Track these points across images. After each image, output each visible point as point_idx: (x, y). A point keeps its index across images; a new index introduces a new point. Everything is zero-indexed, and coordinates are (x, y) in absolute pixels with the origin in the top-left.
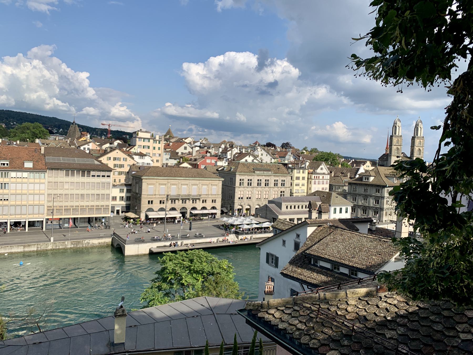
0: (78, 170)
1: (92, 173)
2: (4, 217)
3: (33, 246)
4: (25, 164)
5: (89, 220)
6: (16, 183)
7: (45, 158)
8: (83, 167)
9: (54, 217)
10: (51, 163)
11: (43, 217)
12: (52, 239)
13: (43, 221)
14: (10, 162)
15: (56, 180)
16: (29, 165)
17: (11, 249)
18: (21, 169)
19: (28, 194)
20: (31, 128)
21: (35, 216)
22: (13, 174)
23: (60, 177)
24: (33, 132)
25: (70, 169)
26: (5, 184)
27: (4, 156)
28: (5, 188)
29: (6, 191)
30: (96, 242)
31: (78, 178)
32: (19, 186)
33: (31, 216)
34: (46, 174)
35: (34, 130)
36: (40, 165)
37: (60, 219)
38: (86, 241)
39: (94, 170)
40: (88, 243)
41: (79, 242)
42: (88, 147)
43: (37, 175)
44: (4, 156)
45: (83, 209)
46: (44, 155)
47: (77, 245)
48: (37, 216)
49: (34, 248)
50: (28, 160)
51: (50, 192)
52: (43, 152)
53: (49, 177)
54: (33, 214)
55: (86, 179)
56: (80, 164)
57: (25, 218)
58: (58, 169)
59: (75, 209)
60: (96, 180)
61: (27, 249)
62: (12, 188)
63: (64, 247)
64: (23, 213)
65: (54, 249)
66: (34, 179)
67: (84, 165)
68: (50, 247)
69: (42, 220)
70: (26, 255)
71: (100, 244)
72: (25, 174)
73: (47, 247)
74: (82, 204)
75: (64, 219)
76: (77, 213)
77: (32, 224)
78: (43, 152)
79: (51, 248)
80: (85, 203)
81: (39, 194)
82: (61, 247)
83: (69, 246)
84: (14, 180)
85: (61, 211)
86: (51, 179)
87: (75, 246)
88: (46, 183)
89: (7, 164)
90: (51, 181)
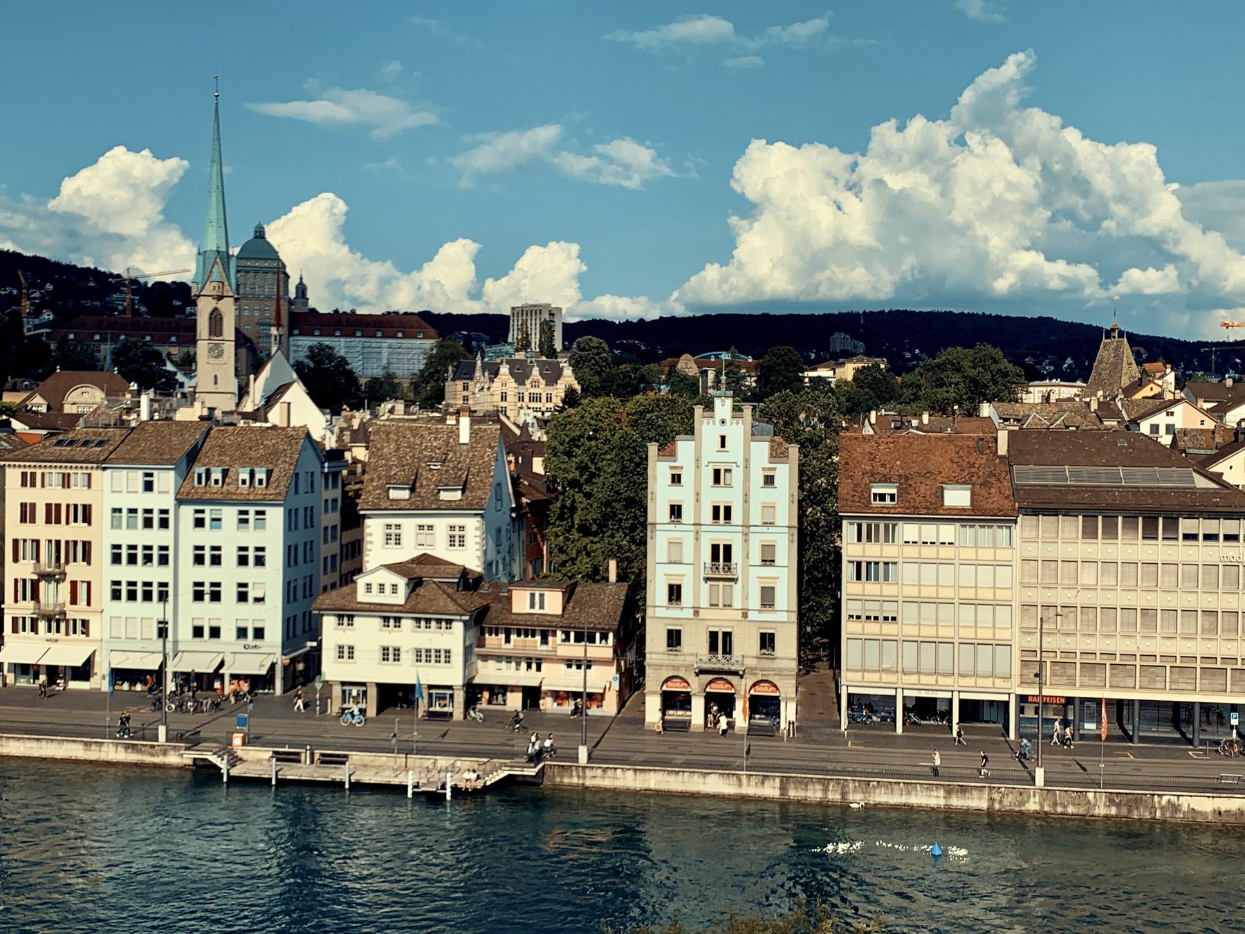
0: (1130, 518)
1: (1185, 525)
2: (886, 678)
3: (975, 793)
4: (947, 494)
5: (1178, 714)
6: (920, 562)
7: (1011, 472)
8: (1150, 502)
9: (1046, 692)
10: (1033, 490)
11: (1005, 686)
12: (1040, 774)
13: (1007, 704)
14: (899, 489)
15: (1051, 551)
16: (957, 497)
17: (909, 793)
18: (934, 512)
19: (957, 601)
20: (966, 364)
21: (981, 682)
22: (909, 531)
23: (1062, 538)
24: (974, 381)
25: (1097, 511)
26: (886, 564)
27: (881, 470)
28: (886, 578)
29: (889, 590)
30: (1205, 805)
31: (1129, 547)
32: (928, 571)
33: (969, 682)
34: (1017, 530)
35: (973, 373)
36: (996, 499)
37: (1070, 700)
38: (1165, 799)
39: (1191, 515)
40: (1175, 808)
41: (1138, 801)
42: (1170, 420)
43: (985, 533)
44: (881, 470)
45: (1151, 667)
46: (1008, 461)
47: (1130, 811)
48: (988, 682)
49: (977, 801)
50: (957, 481)
51: (1033, 596)
52: (1002, 449)
53: (1024, 540)
54: (975, 675)
55: (1160, 550)
56: (1136, 491)
57: (954, 688)
58: (1054, 512)
59: (1122, 667)
60: (1202, 552)
61: (957, 802)
62: (908, 581)
63: (1081, 810)
64: (941, 668)
65: (1046, 813)
66: (976, 546)
67: (1151, 492)
68: (1032, 805)
69: (1004, 698)
70: (955, 824)
71: (1224, 819)
72: (948, 532)
73: (1022, 803)
74: (1147, 646)
75: (1083, 700)
76: (1130, 682)
77: (972, 710)
78: (1002, 449)
79: (1036, 807)
80: (1159, 647)
81: (994, 604)
82: (1071, 810)
83: (1101, 811)
84: (911, 551)
85: (1070, 672)
86: (1032, 550)
87: (1124, 811)
88: (1017, 564)
89: (892, 497)
90: (1032, 555)
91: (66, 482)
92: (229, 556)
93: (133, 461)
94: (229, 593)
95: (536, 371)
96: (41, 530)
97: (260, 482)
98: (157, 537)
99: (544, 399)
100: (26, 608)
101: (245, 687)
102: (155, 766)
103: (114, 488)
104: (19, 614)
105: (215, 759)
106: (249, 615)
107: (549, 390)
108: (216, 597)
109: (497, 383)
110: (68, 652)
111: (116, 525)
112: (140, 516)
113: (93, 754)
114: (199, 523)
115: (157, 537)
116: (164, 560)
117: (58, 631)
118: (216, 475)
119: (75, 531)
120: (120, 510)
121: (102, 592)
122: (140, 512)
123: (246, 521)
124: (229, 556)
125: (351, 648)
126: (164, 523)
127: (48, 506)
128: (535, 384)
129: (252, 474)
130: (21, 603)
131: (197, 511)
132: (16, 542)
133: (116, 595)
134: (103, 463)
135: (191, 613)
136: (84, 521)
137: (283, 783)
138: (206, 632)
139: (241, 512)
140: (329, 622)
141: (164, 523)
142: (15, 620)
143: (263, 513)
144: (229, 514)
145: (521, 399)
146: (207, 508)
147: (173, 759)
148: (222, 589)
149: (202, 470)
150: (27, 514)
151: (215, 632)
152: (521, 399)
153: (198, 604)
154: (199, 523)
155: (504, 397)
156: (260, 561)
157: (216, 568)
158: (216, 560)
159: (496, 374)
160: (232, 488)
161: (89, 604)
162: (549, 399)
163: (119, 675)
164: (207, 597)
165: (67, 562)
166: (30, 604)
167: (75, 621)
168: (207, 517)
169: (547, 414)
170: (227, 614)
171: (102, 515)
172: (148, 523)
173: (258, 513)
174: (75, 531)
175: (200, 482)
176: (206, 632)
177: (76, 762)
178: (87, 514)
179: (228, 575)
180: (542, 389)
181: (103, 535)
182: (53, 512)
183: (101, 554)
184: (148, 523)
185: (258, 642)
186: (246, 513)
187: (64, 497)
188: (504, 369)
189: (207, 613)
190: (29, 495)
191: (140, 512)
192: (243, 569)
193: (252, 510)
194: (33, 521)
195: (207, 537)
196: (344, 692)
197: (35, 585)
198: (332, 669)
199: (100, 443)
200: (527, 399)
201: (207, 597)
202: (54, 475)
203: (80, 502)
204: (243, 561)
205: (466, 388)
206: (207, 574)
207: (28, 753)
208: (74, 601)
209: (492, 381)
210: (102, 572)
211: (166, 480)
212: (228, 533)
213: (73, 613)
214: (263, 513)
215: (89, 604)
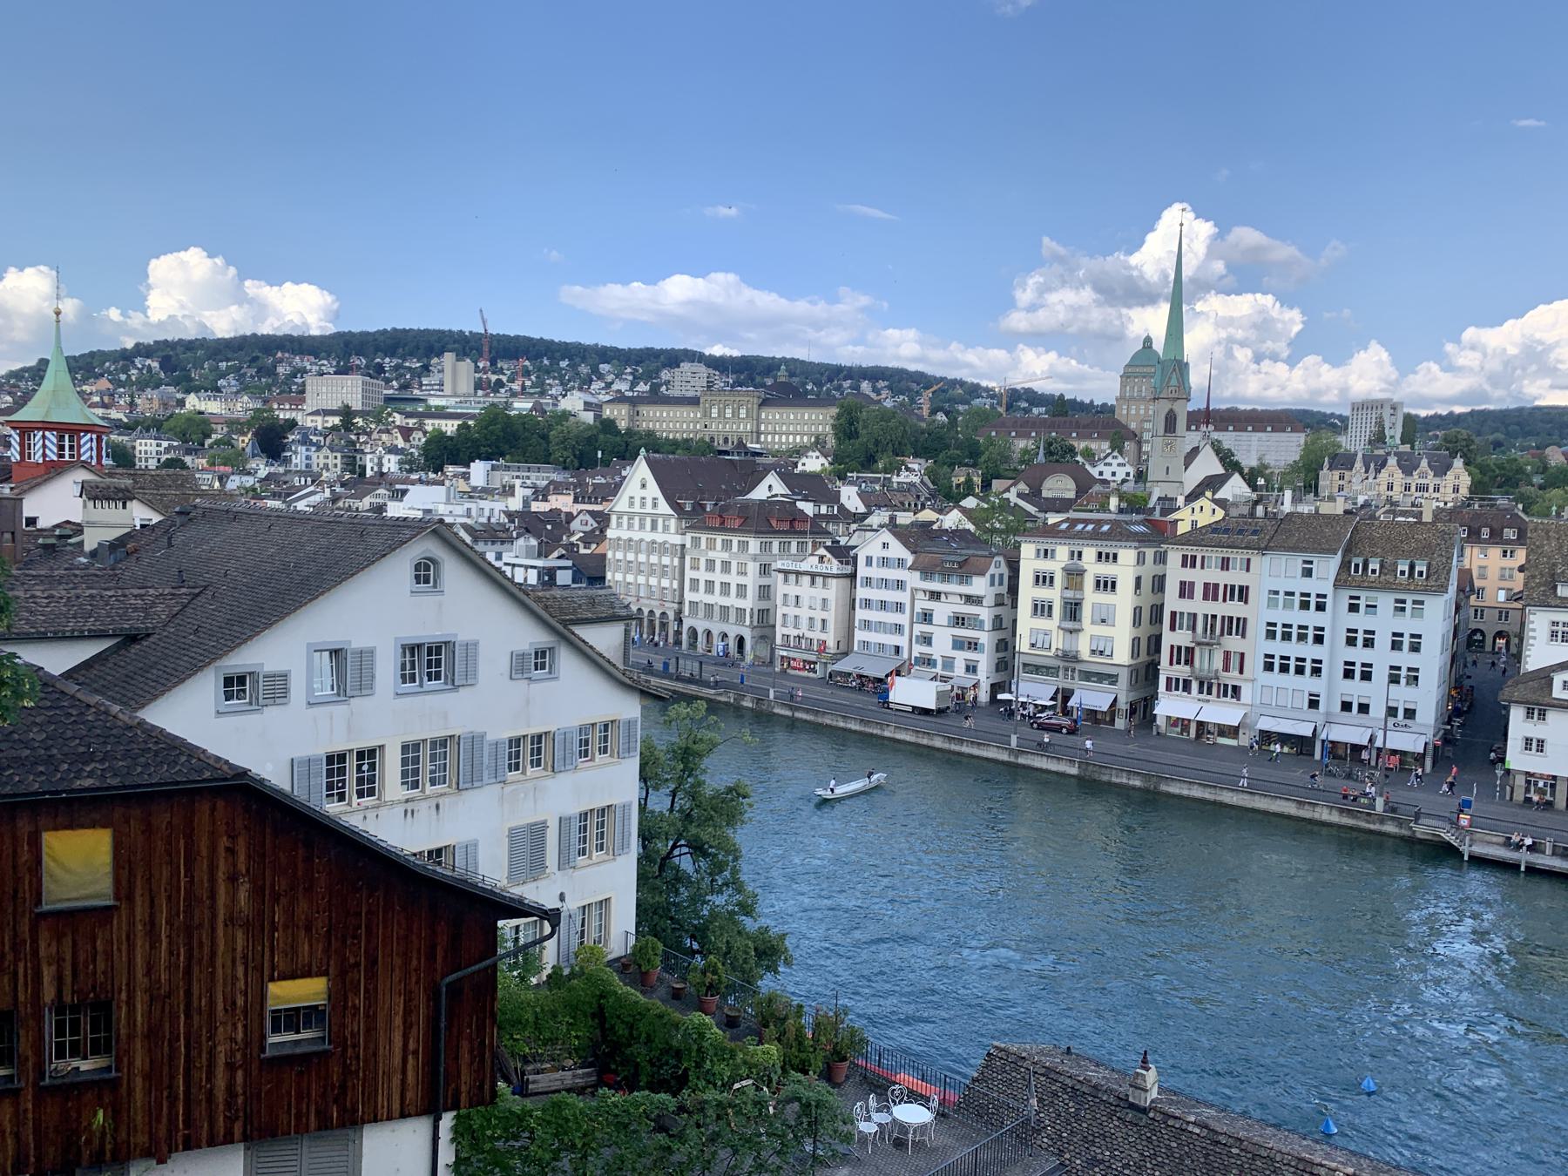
91: (1225, 564)
92: (1383, 640)
93: (1294, 549)
94: (1380, 674)
95: (1424, 463)
96: (1199, 606)
97: (1421, 574)
98: (1312, 618)
99: (1431, 489)
100: (1181, 671)
101: (1395, 760)
102: (1371, 832)
103: (1272, 574)
104: (1174, 675)
105: (1448, 837)
106: (1402, 695)
107: (1437, 481)
108: (1366, 676)
109: (1384, 474)
110: (1221, 712)
111: (1272, 604)
112: (1297, 599)
113: (1306, 813)
114: (1354, 608)
115: (1312, 618)
116: (1319, 639)
117: (1209, 693)
118: (1374, 565)
119: (1234, 609)
120: (1276, 593)
121: (1254, 664)
122: (1297, 595)
123: (1403, 609)
124: (1383, 640)
125: (1541, 743)
126: (1321, 607)
127: (1206, 585)
128: (1423, 475)
129: (1412, 567)
130: (1176, 667)
131: (1352, 598)
132: (1173, 614)
133: (1269, 667)
134: (1263, 549)
135: (1334, 688)
136: (1240, 599)
137: (1532, 870)
138: (1355, 708)
139: (1397, 601)
140: (1517, 715)
141: (1321, 607)
142: (1169, 680)
143: (1422, 603)
144: (1386, 601)
145: (1408, 488)
146: (1363, 594)
147: (1390, 828)
148: (1420, 675)
149: (1360, 561)
150: (1186, 590)
151: (1364, 708)
152: (1408, 488)
153: (1348, 682)
154: (1354, 608)
155: (1390, 487)
156: (1415, 648)
157: (1368, 650)
158: (1369, 643)
159: (1384, 464)
160: (1390, 578)
161: (1241, 672)
162: (1436, 489)
163: (1267, 737)
164: (1403, 681)
165: (1222, 634)
166: (1187, 668)
167: (1226, 686)
168: (1362, 603)
169: (1450, 505)
170: (1376, 692)
171: (1258, 596)
172: (1305, 605)
173: (1415, 602)
174: (1234, 609)
175: (1356, 571)
176: (1355, 708)
177: (1289, 817)
178: (1243, 594)
179: (1381, 658)
180: (1431, 480)
181: (1257, 613)
182: (1211, 592)
183: (1256, 629)
184: (1305, 605)
185: (1408, 722)
186: (1404, 602)
187: (1222, 578)
188: (1392, 461)
189: (1356, 690)
190: (1188, 575)
191: (1297, 595)
192: (1396, 653)
193: (1409, 598)
194: (1191, 597)
195: (1361, 621)
196: (1528, 782)
197: (1190, 651)
198: (1517, 758)
199: (1255, 532)
200: (1413, 488)
201: (1403, 681)
202: (1215, 555)
203: (1237, 584)
204: (1396, 646)
205: (1342, 477)
206: (1359, 655)
207: (1240, 803)
208: (1226, 669)
209: (1378, 471)
210: (1255, 646)
211: (1327, 567)
212: (1384, 619)
213: (1232, 677)
214: (1422, 603)
215: (1241, 672)
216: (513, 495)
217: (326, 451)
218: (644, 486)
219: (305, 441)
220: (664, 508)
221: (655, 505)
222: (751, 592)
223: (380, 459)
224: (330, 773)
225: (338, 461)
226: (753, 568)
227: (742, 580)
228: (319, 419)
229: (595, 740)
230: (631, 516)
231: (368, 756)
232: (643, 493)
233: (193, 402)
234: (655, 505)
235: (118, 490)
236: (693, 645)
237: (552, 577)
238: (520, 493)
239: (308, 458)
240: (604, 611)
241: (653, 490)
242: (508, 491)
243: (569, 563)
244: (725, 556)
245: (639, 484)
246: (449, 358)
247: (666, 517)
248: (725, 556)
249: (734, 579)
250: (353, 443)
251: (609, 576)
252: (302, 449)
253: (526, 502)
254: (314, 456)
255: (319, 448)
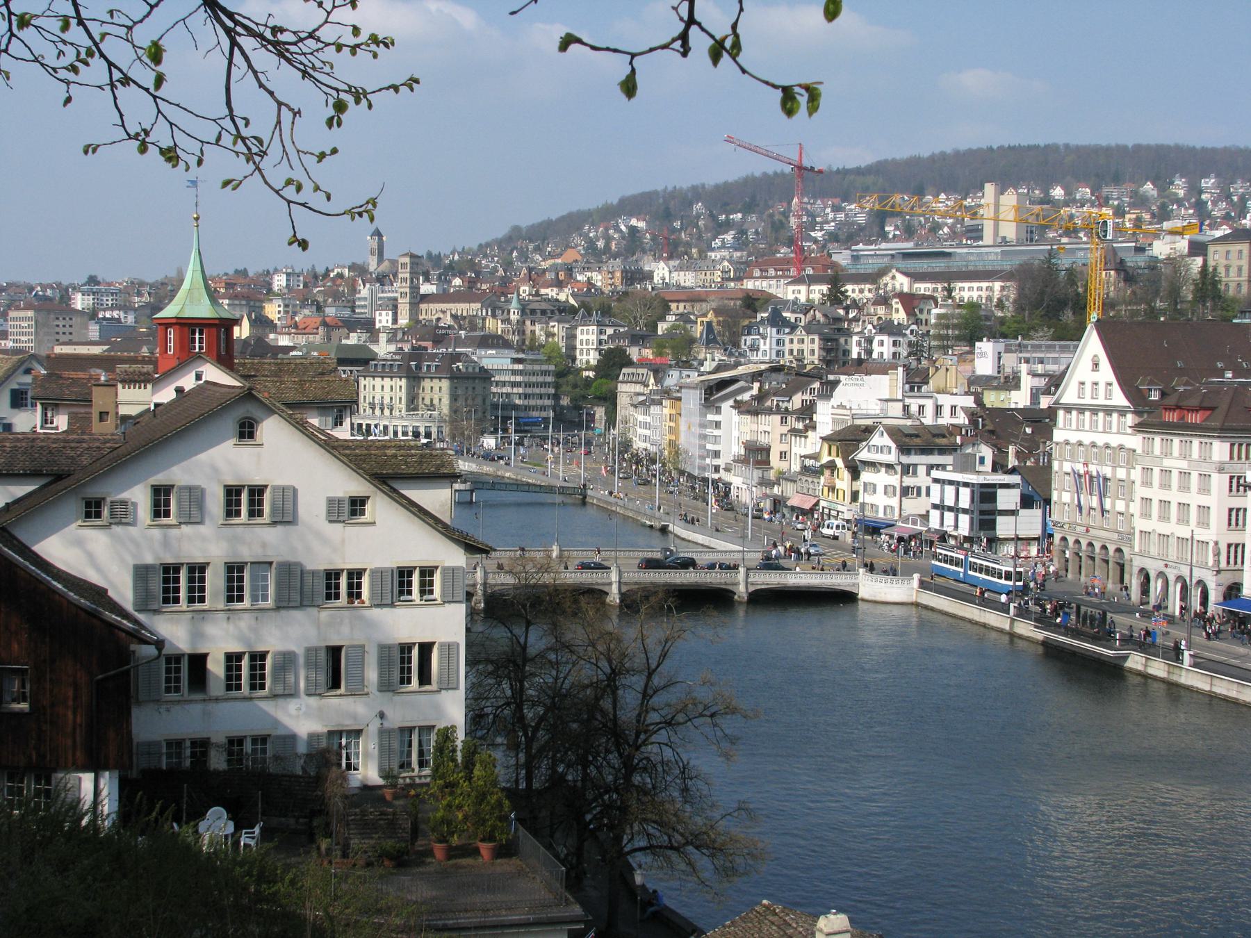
216: (1017, 387)
217: (800, 333)
218: (1096, 365)
219: (777, 321)
220: (1119, 399)
221: (1108, 395)
222: (1218, 518)
223: (870, 341)
224: (166, 580)
225: (816, 346)
226: (1219, 482)
227: (1204, 500)
228: (803, 288)
229: (403, 582)
230: (1081, 409)
231: (198, 570)
232: (1096, 376)
233: (661, 271)
234: (1108, 395)
235: (141, 374)
236: (1145, 590)
237: (992, 498)
238: (1027, 382)
239: (778, 342)
240: (429, 469)
241: (1106, 373)
242: (1012, 382)
243: (1016, 479)
244: (1183, 465)
245: (1090, 369)
246: (989, 188)
247: (1122, 412)
248: (1183, 465)
249: (1194, 499)
250: (839, 320)
251: (1055, 496)
252: (772, 331)
253: (1035, 394)
254: (787, 339)
255: (793, 327)
